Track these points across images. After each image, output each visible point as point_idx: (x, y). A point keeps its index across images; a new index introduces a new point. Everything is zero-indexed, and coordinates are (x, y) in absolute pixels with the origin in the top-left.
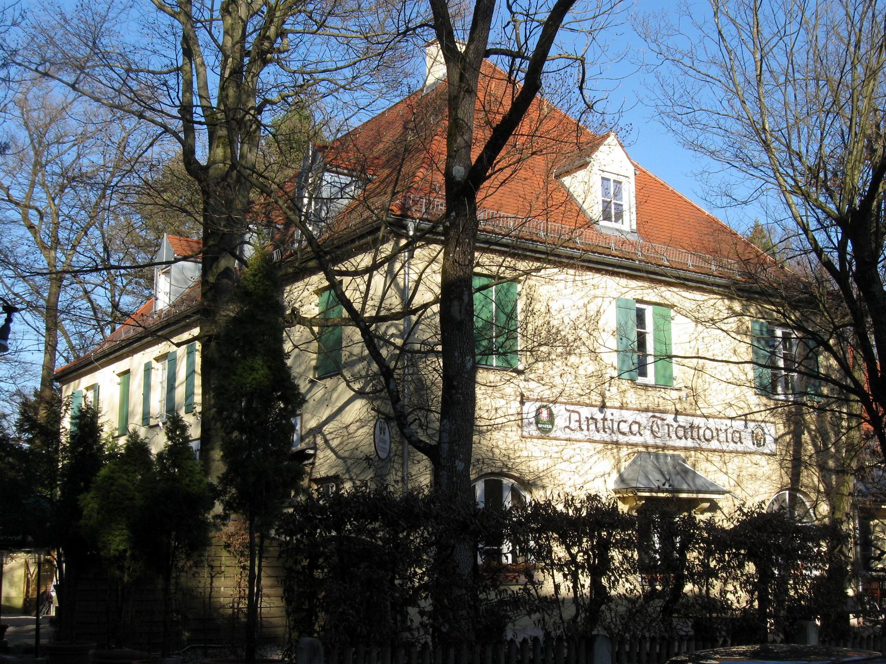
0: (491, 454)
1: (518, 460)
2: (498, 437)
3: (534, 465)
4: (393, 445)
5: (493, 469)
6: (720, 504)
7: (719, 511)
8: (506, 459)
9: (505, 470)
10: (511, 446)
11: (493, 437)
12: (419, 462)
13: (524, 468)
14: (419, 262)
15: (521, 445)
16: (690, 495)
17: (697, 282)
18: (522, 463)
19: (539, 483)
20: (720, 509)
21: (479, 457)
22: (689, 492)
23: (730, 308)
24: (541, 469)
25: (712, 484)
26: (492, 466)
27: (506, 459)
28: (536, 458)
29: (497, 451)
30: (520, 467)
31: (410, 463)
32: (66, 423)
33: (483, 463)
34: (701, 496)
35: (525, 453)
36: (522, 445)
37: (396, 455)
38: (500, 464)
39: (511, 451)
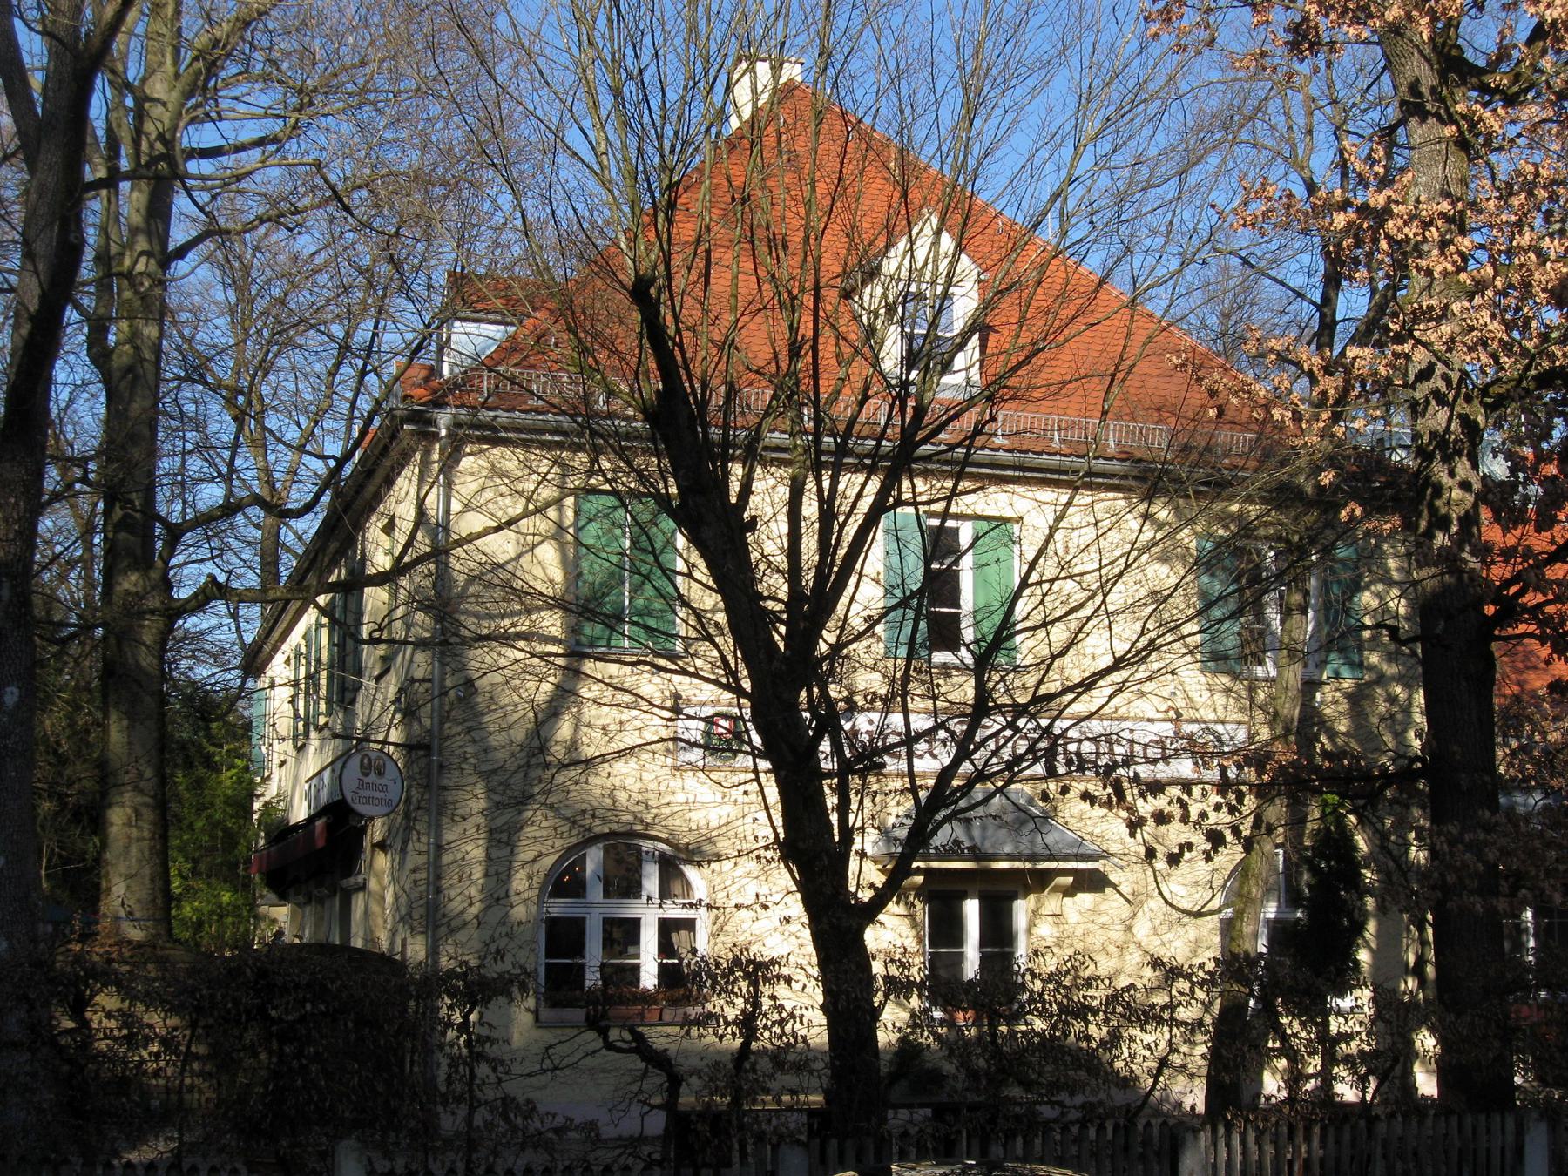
0: (609, 801)
1: (667, 810)
2: (624, 770)
3: (698, 817)
4: (414, 792)
5: (615, 827)
6: (1113, 877)
7: (1109, 890)
8: (641, 808)
9: (638, 827)
10: (653, 786)
11: (614, 771)
12: (464, 819)
13: (677, 822)
14: (469, 478)
15: (672, 784)
16: (1017, 865)
17: (1014, 468)
18: (673, 814)
19: (708, 848)
20: (1115, 886)
21: (585, 806)
22: (1010, 858)
23: (1146, 516)
24: (714, 824)
25: (1080, 842)
26: (611, 821)
27: (641, 808)
28: (705, 805)
29: (622, 796)
30: (670, 822)
31: (445, 820)
32: (257, 806)
33: (594, 816)
34: (1053, 865)
35: (680, 798)
36: (675, 783)
37: (419, 808)
38: (628, 817)
39: (650, 795)
